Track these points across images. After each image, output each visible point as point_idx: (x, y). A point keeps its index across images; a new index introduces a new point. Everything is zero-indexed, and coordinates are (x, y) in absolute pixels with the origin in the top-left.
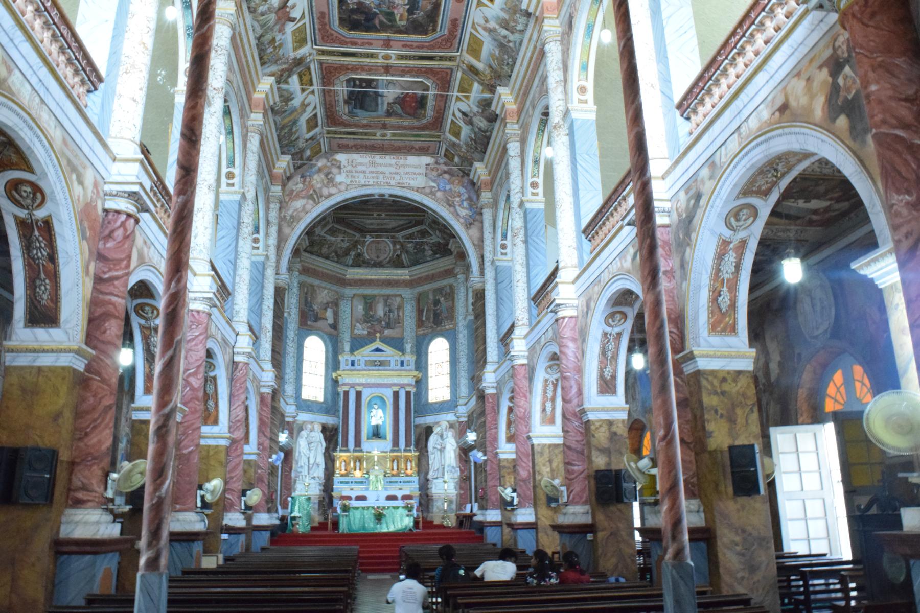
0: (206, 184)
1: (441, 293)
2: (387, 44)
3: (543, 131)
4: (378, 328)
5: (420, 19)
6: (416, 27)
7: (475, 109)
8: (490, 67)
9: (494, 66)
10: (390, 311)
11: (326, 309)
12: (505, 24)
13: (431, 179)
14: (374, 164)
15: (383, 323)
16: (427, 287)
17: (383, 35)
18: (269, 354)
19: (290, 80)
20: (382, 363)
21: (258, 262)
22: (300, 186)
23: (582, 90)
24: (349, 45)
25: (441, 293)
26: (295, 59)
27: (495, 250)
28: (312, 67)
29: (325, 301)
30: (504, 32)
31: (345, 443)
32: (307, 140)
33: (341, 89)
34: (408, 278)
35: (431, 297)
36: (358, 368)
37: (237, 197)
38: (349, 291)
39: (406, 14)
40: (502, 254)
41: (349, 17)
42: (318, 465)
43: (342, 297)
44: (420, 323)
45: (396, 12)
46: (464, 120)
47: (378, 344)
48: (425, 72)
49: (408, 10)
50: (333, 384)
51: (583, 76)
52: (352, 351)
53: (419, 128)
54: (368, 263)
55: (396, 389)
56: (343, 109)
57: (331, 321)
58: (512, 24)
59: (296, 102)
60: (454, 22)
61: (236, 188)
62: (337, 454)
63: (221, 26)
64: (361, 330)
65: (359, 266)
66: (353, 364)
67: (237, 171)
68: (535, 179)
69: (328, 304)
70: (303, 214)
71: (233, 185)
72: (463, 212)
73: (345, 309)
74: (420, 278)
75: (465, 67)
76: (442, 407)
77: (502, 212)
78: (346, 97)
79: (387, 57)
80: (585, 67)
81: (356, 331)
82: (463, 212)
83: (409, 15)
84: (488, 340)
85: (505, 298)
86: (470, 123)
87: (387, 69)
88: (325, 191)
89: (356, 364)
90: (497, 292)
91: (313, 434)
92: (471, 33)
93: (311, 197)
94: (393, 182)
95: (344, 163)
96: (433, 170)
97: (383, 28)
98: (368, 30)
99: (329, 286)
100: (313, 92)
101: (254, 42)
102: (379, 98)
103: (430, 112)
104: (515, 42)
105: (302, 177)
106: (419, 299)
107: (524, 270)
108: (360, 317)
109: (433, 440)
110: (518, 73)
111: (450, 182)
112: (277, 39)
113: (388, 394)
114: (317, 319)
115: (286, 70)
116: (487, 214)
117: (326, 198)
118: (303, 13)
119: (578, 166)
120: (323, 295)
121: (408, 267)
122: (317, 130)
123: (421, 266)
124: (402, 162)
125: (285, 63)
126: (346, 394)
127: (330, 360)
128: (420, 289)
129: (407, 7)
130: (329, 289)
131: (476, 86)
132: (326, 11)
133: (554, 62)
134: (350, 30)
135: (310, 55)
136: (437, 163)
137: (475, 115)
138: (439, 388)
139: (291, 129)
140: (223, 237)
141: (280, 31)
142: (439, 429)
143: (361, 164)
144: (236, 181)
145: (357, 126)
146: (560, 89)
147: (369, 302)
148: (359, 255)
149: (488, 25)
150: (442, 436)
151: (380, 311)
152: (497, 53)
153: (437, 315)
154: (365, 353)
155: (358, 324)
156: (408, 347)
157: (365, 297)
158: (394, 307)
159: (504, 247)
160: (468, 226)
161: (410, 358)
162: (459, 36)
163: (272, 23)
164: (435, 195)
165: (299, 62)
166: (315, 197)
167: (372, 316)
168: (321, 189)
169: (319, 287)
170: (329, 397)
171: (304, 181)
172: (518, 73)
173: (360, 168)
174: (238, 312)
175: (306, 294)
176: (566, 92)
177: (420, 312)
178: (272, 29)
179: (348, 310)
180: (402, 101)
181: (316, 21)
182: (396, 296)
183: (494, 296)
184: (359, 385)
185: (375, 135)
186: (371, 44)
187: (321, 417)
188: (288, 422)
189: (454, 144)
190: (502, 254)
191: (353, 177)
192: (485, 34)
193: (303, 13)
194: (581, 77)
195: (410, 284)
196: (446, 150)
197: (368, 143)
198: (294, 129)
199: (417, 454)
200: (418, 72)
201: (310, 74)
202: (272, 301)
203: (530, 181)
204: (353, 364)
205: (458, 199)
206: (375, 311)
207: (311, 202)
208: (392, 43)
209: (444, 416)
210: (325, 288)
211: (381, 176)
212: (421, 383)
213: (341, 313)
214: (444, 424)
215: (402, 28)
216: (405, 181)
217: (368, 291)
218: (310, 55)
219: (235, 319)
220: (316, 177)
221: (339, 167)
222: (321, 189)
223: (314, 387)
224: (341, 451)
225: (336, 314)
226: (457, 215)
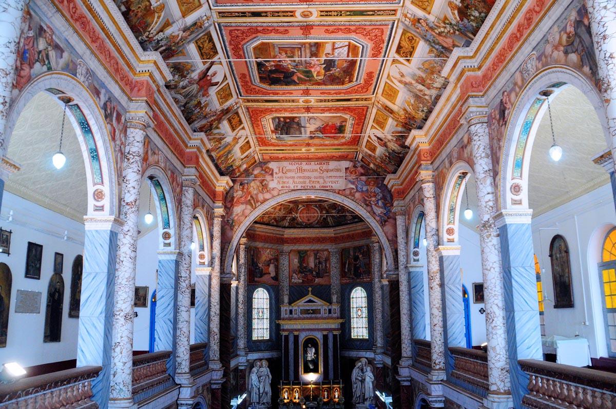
0: (122, 314)
1: (360, 251)
2: (306, 92)
3: (460, 185)
4: (310, 277)
5: (337, 74)
6: (333, 80)
7: (390, 137)
8: (405, 110)
9: (409, 110)
10: (320, 263)
11: (269, 265)
12: (422, 81)
13: (350, 181)
14: (301, 170)
15: (314, 273)
16: (347, 245)
17: (303, 87)
18: (218, 355)
19: (220, 126)
20: (315, 312)
21: (204, 276)
22: (240, 193)
23: (516, 189)
24: (271, 95)
25: (360, 251)
26: (222, 111)
27: (407, 256)
28: (240, 112)
29: (268, 259)
30: (420, 87)
31: (287, 377)
32: (242, 159)
33: (268, 124)
34: (333, 235)
35: (352, 253)
36: (295, 316)
37: (174, 257)
38: (287, 248)
39: (323, 71)
40: (415, 260)
41: (269, 76)
42: (267, 394)
43: (282, 252)
44: (343, 274)
45: (313, 70)
46: (379, 142)
47: (310, 297)
48: (343, 110)
49: (325, 68)
50: (275, 328)
51: (517, 174)
52: (290, 303)
53: (338, 145)
54: (301, 224)
55: (325, 333)
56: (271, 136)
57: (273, 274)
58: (428, 81)
59: (229, 139)
60: (370, 75)
61: (172, 248)
62: (281, 386)
63: (132, 130)
64: (297, 279)
65: (295, 227)
66: (291, 312)
67: (172, 231)
68: (451, 226)
69: (270, 260)
70: (242, 218)
71: (169, 245)
72: (378, 211)
73: (284, 262)
74: (343, 237)
75: (380, 106)
77: (414, 226)
78: (273, 129)
79: (306, 101)
80: (519, 165)
81: (293, 280)
82: (378, 211)
83: (326, 71)
84: (403, 337)
85: (417, 301)
86: (385, 145)
87: (308, 109)
88: (261, 197)
89: (293, 313)
90: (410, 294)
91: (262, 369)
92: (386, 83)
93: (249, 203)
94: (317, 186)
95: (276, 170)
96: (351, 173)
97: (302, 82)
98: (287, 84)
99: (270, 246)
100: (243, 128)
101: (178, 112)
102: (302, 129)
103: (348, 134)
104: (431, 96)
105: (241, 184)
106: (343, 253)
107: (441, 314)
108: (296, 268)
109: (355, 373)
110: (433, 124)
111: (367, 183)
112: (202, 102)
113: (319, 336)
114: (262, 274)
115: (215, 120)
116: (400, 221)
117: (262, 203)
118: (225, 76)
119: (514, 283)
120: (266, 255)
121: (333, 227)
122: (251, 150)
123: (344, 227)
124: (325, 167)
125: (214, 116)
126: (287, 337)
127: (274, 306)
128: (342, 245)
129: (324, 66)
130: (271, 248)
131: (390, 121)
132: (246, 72)
133: (481, 149)
134: (270, 85)
135: (236, 104)
136: (355, 166)
137: (389, 141)
138: (359, 329)
139: (227, 157)
140: (163, 297)
141: (203, 96)
142: (360, 364)
143: (290, 171)
144: (172, 240)
145: (286, 146)
146: (489, 180)
147: (302, 256)
148: (294, 219)
149: (403, 79)
150: (362, 370)
151: (312, 263)
152: (412, 101)
153: (356, 269)
154: (301, 304)
155: (294, 275)
156: (334, 298)
157: (299, 252)
158: (322, 260)
159: (416, 254)
160: (383, 223)
161: (335, 307)
162: (374, 84)
163: (195, 92)
164: (353, 196)
165: (226, 111)
166: (253, 202)
167: (305, 268)
168: (257, 195)
169: (263, 248)
170: (274, 335)
171: (243, 189)
172: (433, 124)
173: (289, 174)
174: (180, 364)
175: (253, 256)
176: (495, 185)
177: (343, 265)
178: (196, 96)
179: (286, 263)
180: (323, 130)
181: (238, 80)
182: (323, 250)
183: (407, 297)
184: (296, 330)
185: (301, 150)
186: (291, 93)
188: (241, 370)
189: (370, 156)
190: (415, 260)
191: (284, 183)
192: (402, 86)
193: (225, 76)
194: (515, 174)
195: (333, 240)
196: (363, 157)
197: (295, 155)
198: (229, 156)
200: (337, 110)
201: (239, 116)
202: (218, 307)
203: (446, 227)
204: (291, 312)
205: (373, 199)
206: (308, 264)
207: (249, 207)
208: (310, 92)
210: (268, 248)
211: (308, 181)
212: (346, 326)
213: (281, 266)
215: (320, 81)
216: (328, 184)
217: (302, 247)
218: (236, 104)
219: (178, 371)
220: (252, 184)
221: (272, 174)
222: (257, 195)
223: (261, 330)
224: (284, 384)
225: (277, 268)
226: (373, 214)
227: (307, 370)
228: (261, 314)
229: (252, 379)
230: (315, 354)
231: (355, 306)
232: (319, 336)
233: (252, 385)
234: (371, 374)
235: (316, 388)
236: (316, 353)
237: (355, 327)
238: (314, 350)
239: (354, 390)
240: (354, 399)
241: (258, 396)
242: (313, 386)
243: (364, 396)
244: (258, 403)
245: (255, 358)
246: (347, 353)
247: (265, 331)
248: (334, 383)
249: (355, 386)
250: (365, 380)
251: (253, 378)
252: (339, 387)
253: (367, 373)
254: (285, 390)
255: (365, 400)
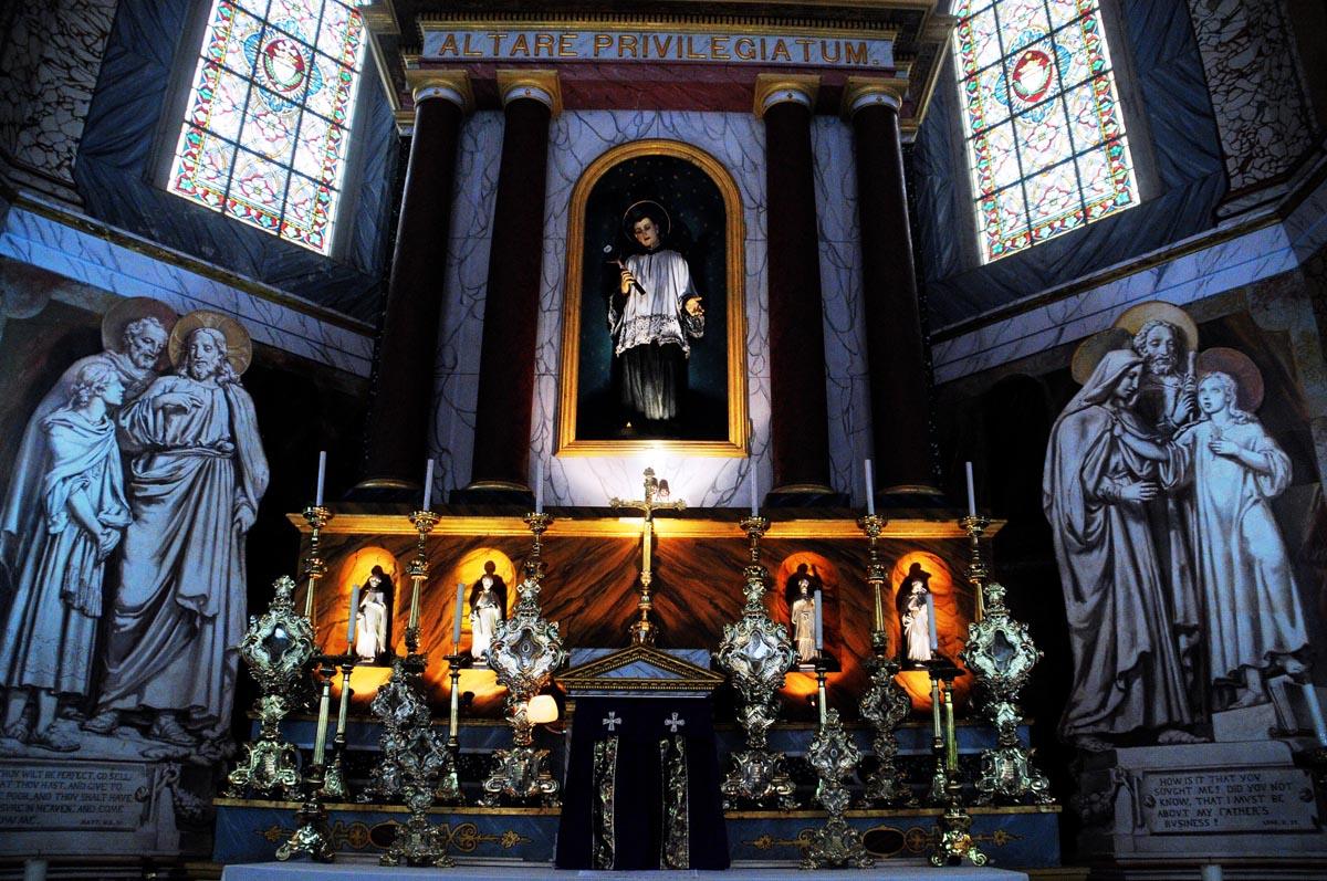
55: (784, 91)
62: (313, 520)
76: (1095, 250)
109: (1074, 446)
113: (729, 145)
142: (1118, 360)
150: (1148, 412)
170: (370, 232)
187: (290, 318)
199: (996, 526)
209: (1142, 282)
214: (1156, 325)
227: (606, 417)
228: (283, 69)
229: (47, 457)
230: (685, 298)
231: (988, 54)
232: (729, 145)
233: (37, 509)
234: (1254, 430)
235: (699, 545)
236: (710, 284)
237: (1005, 173)
238: (680, 274)
239: (1075, 613)
240: (1088, 695)
241: (83, 633)
242: (668, 529)
243: (1201, 652)
244: (82, 706)
245: (128, 289)
246: (965, 344)
247: (302, 191)
248: (891, 507)
249: (1088, 567)
250: (1186, 493)
251: (63, 440)
252: (953, 553)
253: (1203, 430)
254: (363, 567)
255: (1209, 692)
